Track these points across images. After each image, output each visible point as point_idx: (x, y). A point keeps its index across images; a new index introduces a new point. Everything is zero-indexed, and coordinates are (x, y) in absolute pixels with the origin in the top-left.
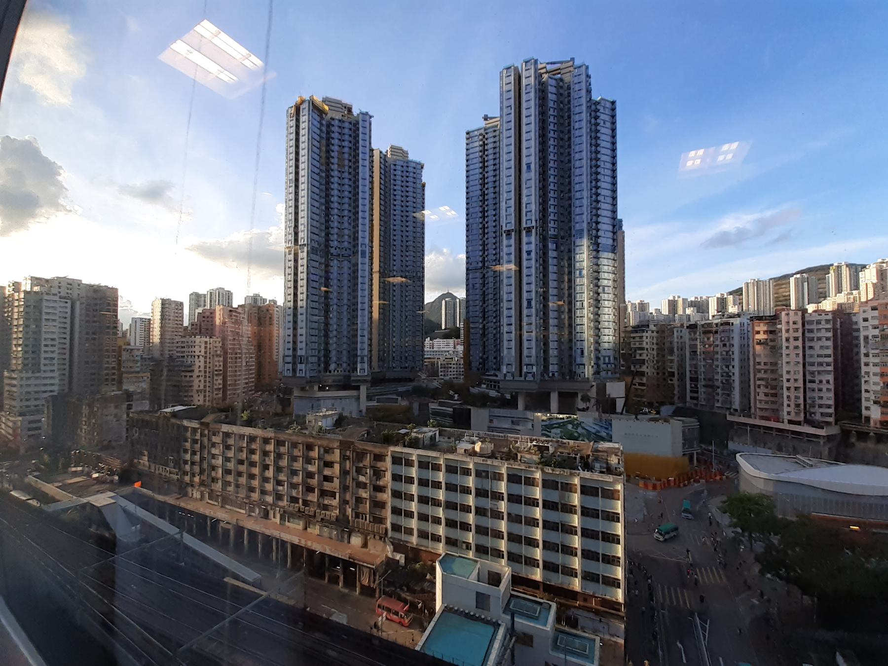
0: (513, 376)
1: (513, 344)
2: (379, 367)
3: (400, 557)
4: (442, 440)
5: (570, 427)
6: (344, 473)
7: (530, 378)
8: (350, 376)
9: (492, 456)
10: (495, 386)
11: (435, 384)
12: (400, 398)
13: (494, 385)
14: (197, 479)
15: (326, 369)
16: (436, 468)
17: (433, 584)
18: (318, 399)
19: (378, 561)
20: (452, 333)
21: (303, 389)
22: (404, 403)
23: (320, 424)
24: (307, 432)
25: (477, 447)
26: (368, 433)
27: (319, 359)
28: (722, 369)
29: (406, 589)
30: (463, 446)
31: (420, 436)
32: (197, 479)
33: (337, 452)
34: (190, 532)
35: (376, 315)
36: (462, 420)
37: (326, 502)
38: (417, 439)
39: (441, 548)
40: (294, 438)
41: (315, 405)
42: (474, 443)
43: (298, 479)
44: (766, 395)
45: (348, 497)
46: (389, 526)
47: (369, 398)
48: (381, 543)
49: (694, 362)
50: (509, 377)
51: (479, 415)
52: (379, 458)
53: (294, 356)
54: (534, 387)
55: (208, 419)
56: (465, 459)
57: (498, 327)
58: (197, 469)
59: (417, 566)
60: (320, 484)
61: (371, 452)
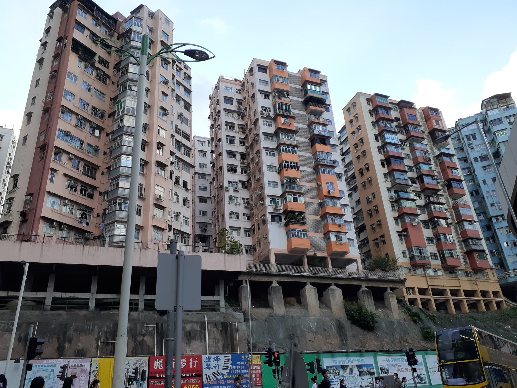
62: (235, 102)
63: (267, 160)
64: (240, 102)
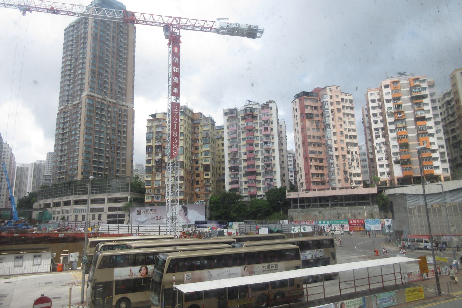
28: (262, 154)
44: (317, 167)
49: (235, 150)
62: (377, 101)
63: (392, 135)
64: (379, 100)
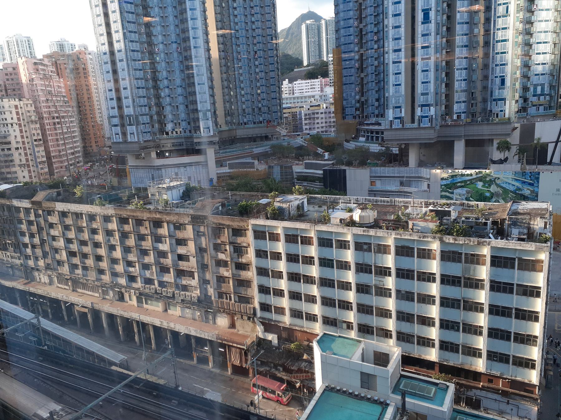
0: (402, 122)
1: (402, 78)
2: (227, 123)
3: (272, 337)
4: (311, 208)
5: (480, 185)
6: (201, 251)
7: (426, 123)
8: (191, 137)
9: (376, 225)
10: (377, 138)
11: (299, 141)
12: (256, 162)
13: (376, 136)
14: (41, 263)
15: (162, 131)
16: (307, 241)
17: (311, 363)
18: (159, 168)
19: (249, 341)
20: (318, 71)
21: (138, 157)
22: (261, 167)
23: (165, 197)
24: (152, 207)
25: (356, 216)
26: (223, 205)
27: (151, 117)
29: (281, 369)
30: (338, 215)
31: (284, 206)
32: (41, 263)
33: (190, 228)
34: (46, 316)
35: (215, 53)
36: (335, 183)
37: (184, 282)
38: (281, 210)
39: (318, 328)
40: (139, 215)
41: (156, 173)
42: (351, 210)
43: (150, 259)
45: (208, 276)
46: (257, 306)
47: (220, 163)
48: (251, 324)
50: (397, 125)
51: (357, 177)
52: (238, 232)
53: (122, 117)
54: (431, 135)
55: (40, 196)
56: (340, 230)
57: (381, 56)
58: (39, 252)
59: (292, 346)
60: (175, 265)
61: (228, 227)
